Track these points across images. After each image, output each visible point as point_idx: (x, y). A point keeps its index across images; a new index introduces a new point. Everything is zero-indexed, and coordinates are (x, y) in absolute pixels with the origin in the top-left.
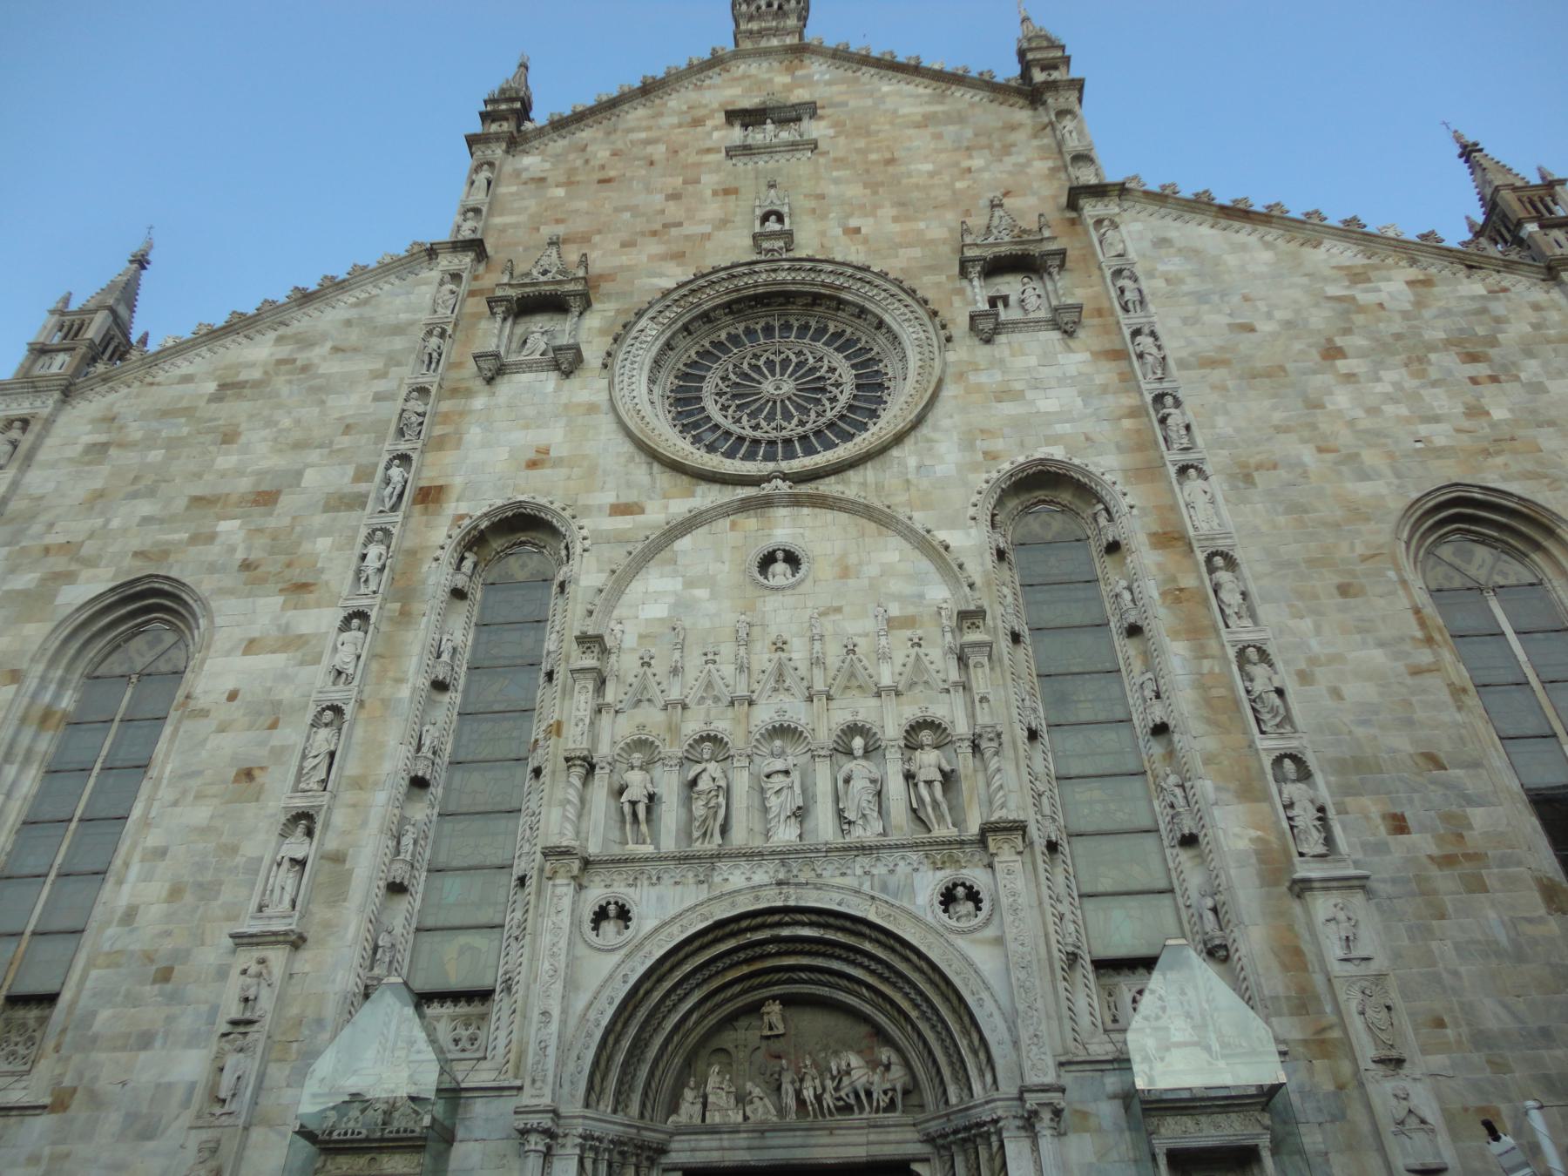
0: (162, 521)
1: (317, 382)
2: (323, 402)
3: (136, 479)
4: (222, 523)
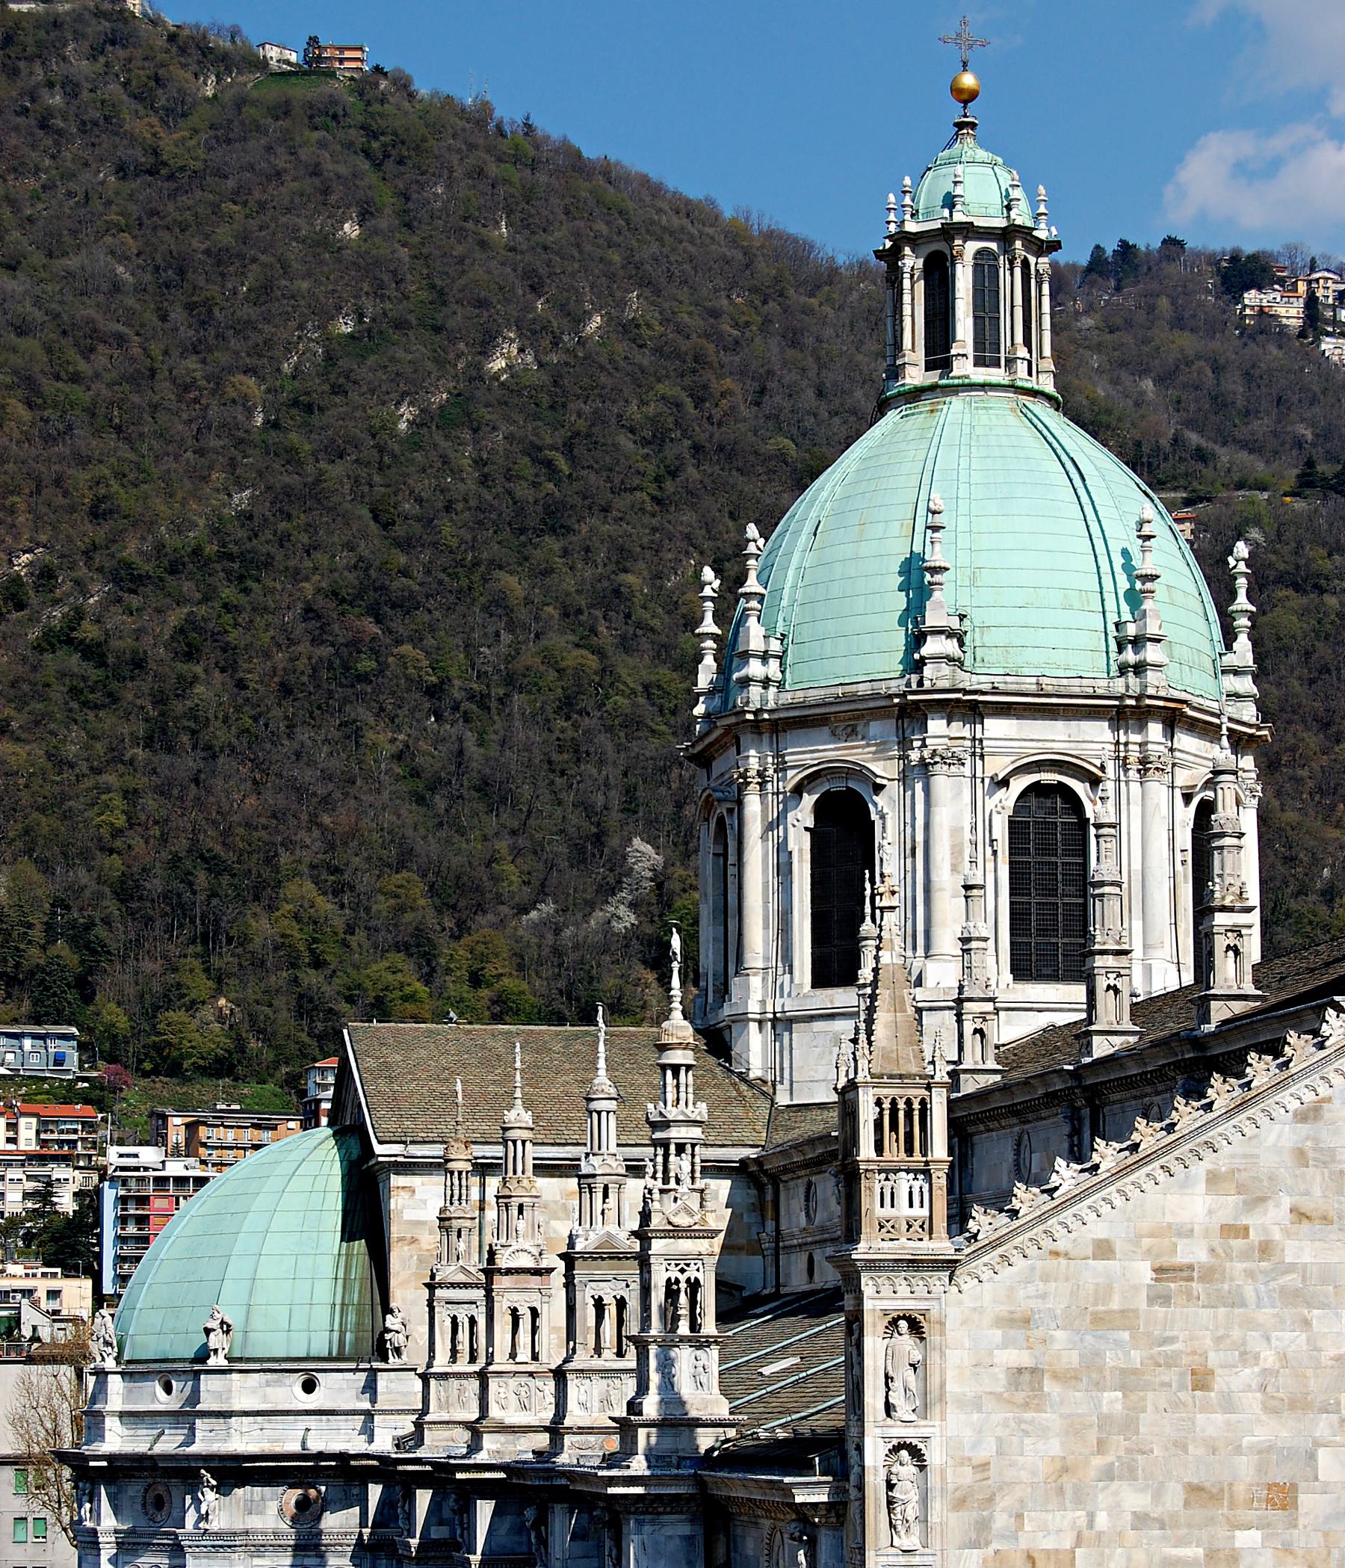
0: (1162, 1528)
1: (1290, 1280)
2: (1306, 1323)
3: (1100, 1443)
4: (1237, 1533)
